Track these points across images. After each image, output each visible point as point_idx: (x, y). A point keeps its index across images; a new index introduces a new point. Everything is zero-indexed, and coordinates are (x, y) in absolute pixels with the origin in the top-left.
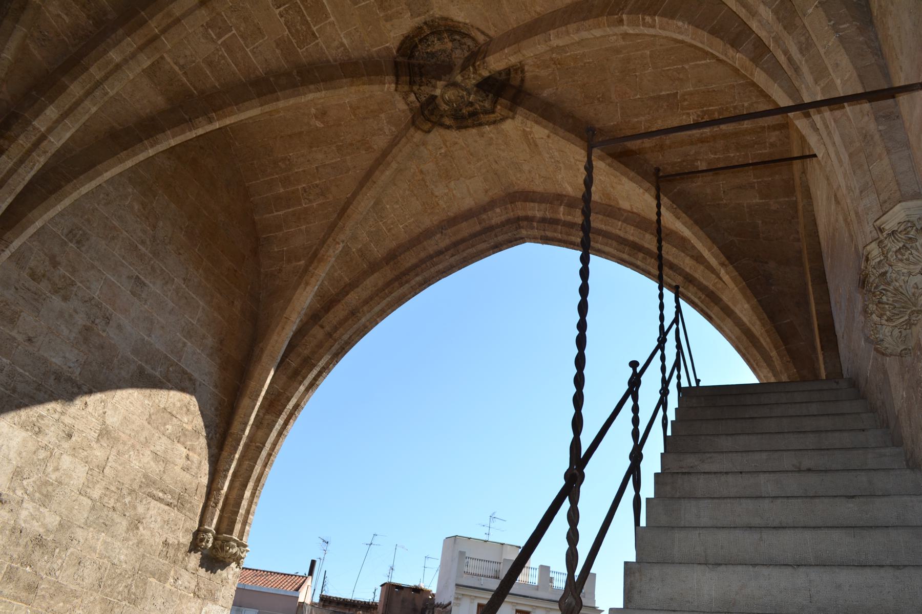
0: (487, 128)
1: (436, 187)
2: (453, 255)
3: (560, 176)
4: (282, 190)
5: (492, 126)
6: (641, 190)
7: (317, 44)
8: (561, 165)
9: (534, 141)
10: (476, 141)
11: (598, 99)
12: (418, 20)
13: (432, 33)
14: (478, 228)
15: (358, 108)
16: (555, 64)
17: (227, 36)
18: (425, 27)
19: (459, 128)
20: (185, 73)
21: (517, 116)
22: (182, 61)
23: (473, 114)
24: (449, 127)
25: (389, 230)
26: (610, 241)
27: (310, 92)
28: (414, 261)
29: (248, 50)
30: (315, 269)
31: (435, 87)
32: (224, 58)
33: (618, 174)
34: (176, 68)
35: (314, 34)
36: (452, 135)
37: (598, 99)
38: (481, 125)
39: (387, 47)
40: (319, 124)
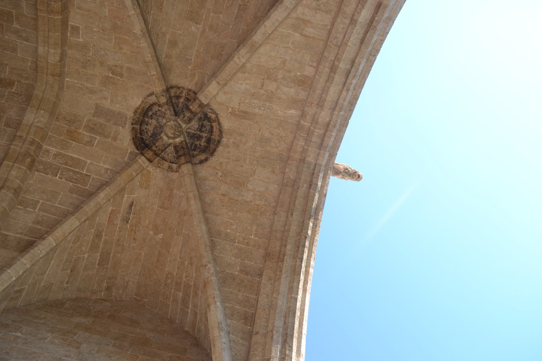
0: (224, 140)
1: (243, 196)
2: (292, 214)
3: (279, 112)
4: (181, 294)
5: (224, 135)
6: (263, 27)
7: (93, 178)
8: (268, 104)
9: (242, 112)
10: (229, 152)
11: (222, 51)
12: (128, 126)
13: (141, 125)
14: (289, 189)
15: (164, 203)
16: (194, 70)
17: (39, 206)
18: (134, 126)
19: (212, 154)
20: (25, 235)
21: (200, 98)
22: (20, 231)
23: (209, 141)
24: (206, 160)
25: (248, 244)
26: (326, 88)
27: (99, 193)
28: (278, 244)
29: (56, 205)
30: (207, 293)
31: (161, 138)
32: (45, 216)
33: (250, 41)
34: (19, 236)
35: (87, 175)
36: (213, 161)
37: (222, 51)
38: (219, 142)
39: (131, 152)
40: (160, 236)
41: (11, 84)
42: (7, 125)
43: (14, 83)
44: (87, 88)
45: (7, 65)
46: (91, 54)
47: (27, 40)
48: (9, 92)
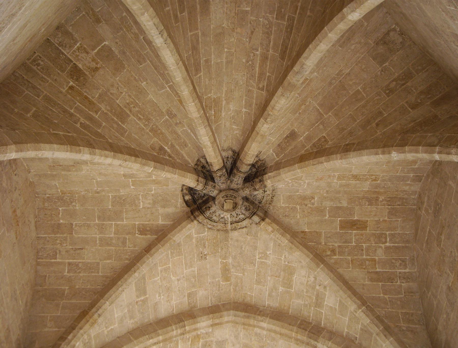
41: (227, 279)
42: (189, 295)
43: (229, 281)
44: (238, 334)
45: (244, 275)
46: (268, 342)
47: (270, 295)
48: (219, 281)
